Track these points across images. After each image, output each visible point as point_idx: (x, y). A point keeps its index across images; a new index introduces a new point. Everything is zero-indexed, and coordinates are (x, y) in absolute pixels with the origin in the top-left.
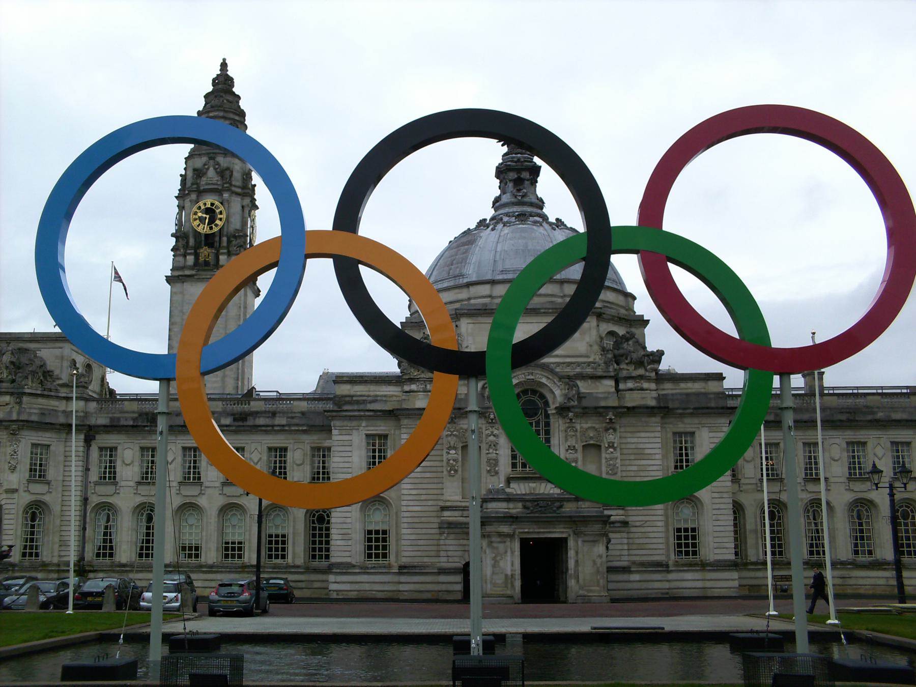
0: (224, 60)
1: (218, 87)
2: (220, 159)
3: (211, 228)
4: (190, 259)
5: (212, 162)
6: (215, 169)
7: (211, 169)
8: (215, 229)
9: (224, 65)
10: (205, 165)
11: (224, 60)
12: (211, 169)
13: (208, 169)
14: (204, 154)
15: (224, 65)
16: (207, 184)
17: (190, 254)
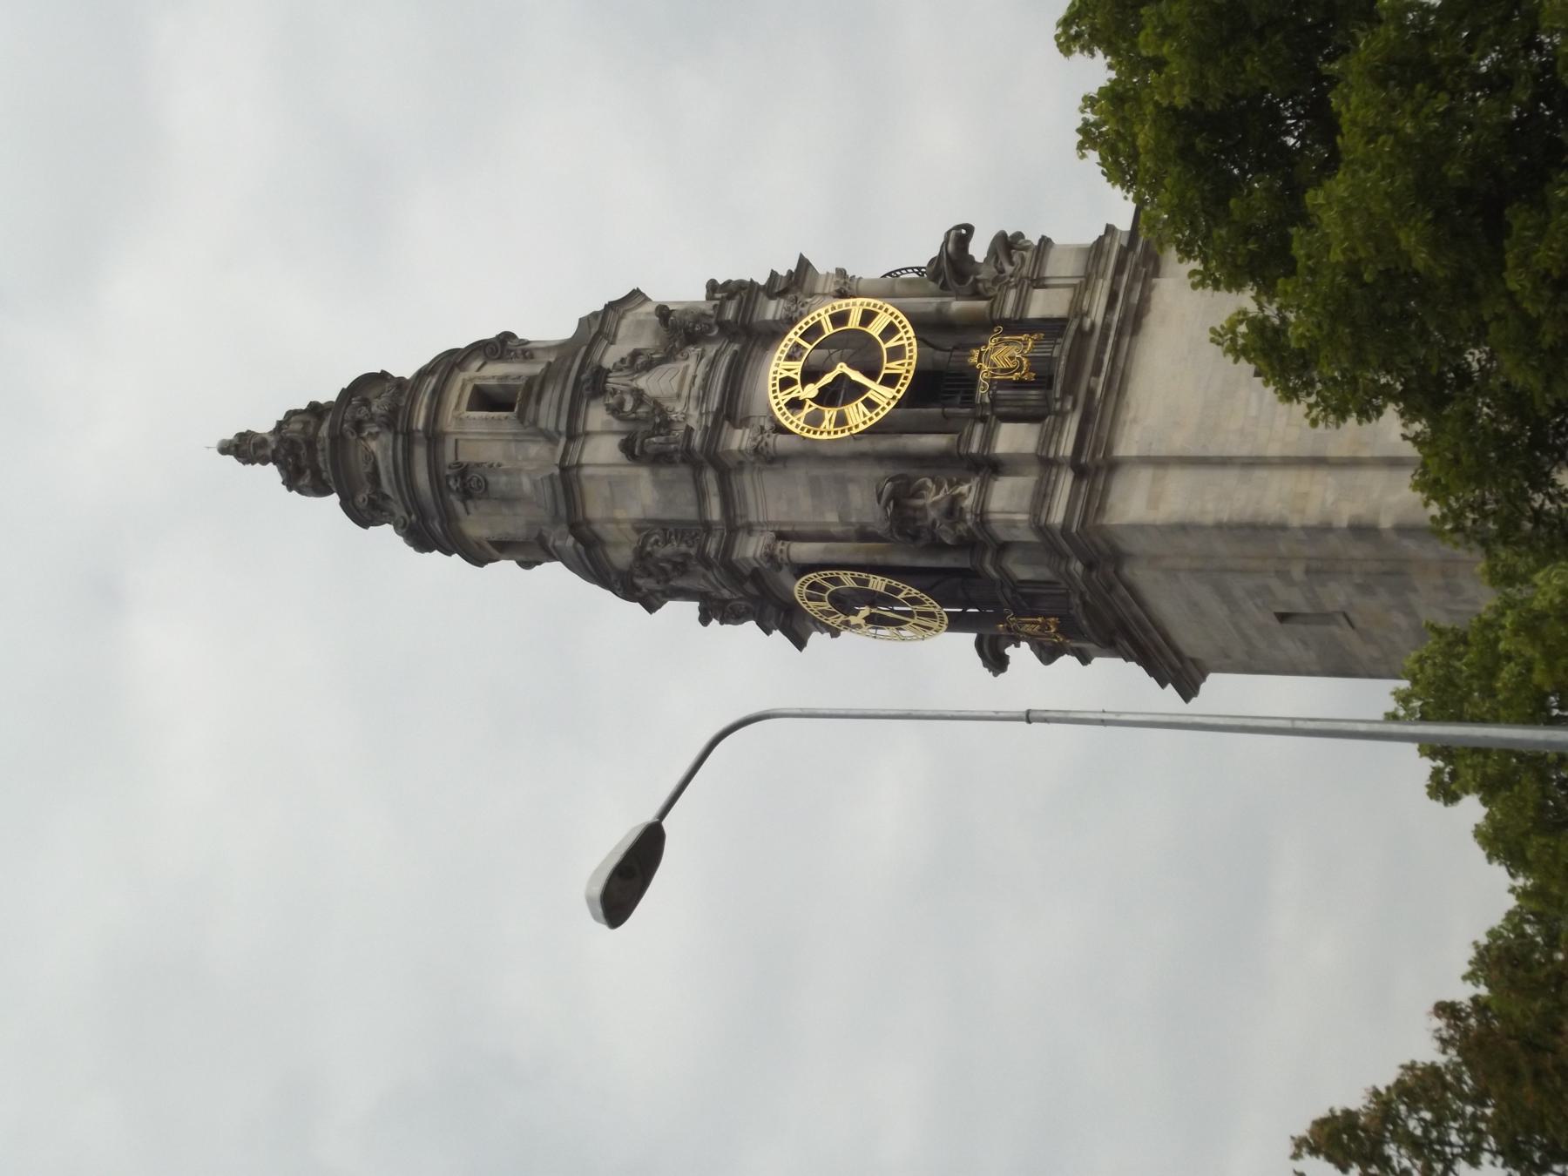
0: (225, 449)
1: (327, 474)
2: (611, 356)
3: (890, 381)
4: (1013, 438)
5: (614, 381)
6: (649, 366)
7: (642, 382)
8: (907, 336)
9: (244, 448)
10: (616, 411)
11: (225, 449)
12: (642, 382)
13: (639, 395)
14: (574, 414)
15: (244, 448)
16: (703, 398)
17: (988, 438)
